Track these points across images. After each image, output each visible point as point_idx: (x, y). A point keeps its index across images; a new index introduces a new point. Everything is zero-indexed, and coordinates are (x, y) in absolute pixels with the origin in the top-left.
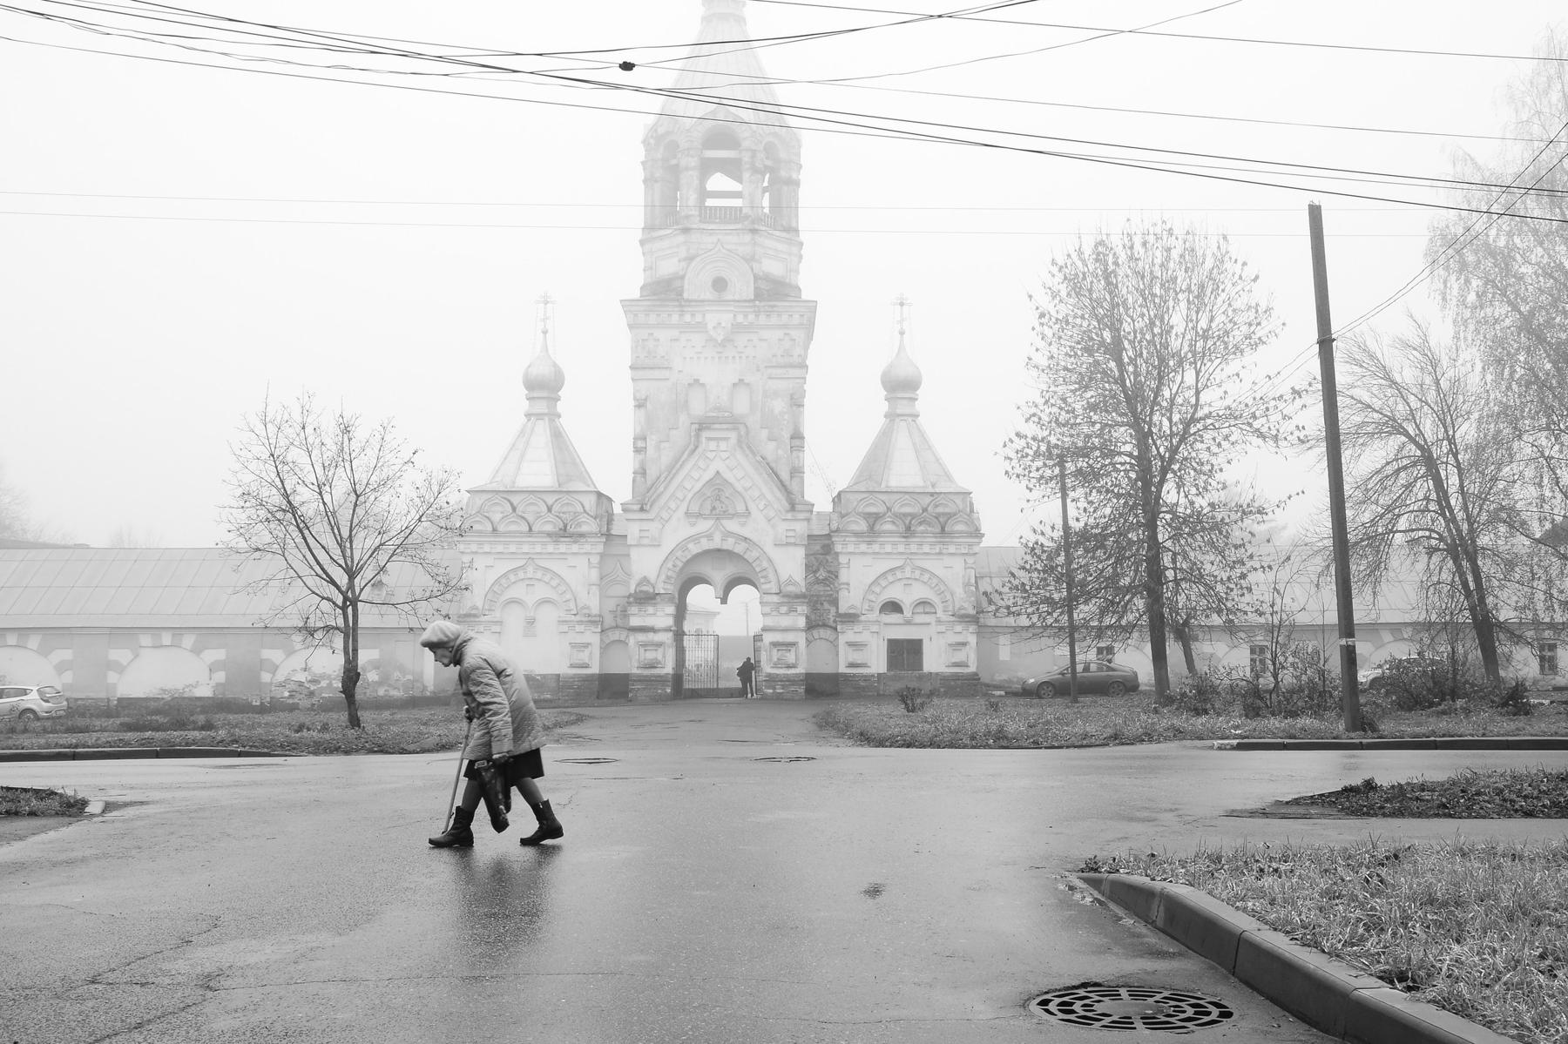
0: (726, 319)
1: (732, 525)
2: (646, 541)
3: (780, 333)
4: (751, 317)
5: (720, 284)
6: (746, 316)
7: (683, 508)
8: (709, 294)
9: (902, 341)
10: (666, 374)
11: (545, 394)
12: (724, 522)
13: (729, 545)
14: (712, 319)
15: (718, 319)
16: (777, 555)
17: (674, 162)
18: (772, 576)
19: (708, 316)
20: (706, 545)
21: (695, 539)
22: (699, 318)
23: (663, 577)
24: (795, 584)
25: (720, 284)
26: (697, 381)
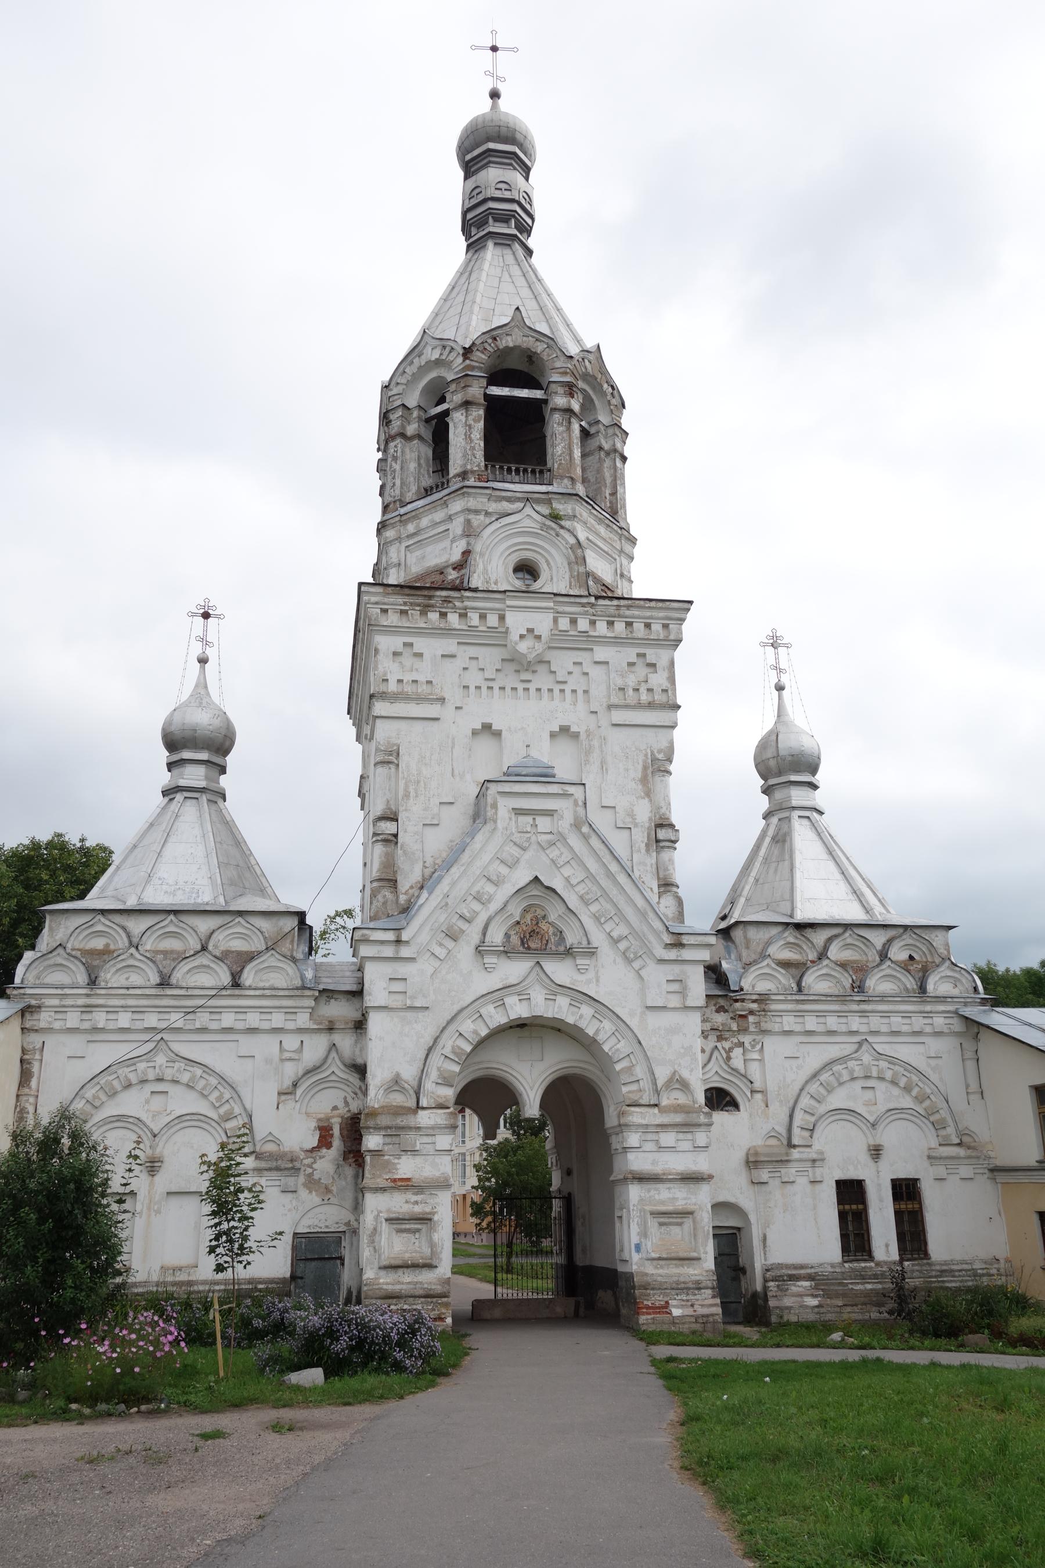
3: (630, 654)
4: (583, 624)
5: (526, 569)
6: (574, 622)
13: (561, 1009)
14: (517, 622)
16: (653, 1029)
17: (440, 409)
18: (640, 1072)
19: (511, 618)
20: (518, 1010)
21: (497, 996)
22: (493, 620)
23: (434, 1075)
24: (684, 1086)
25: (526, 569)
26: (487, 727)
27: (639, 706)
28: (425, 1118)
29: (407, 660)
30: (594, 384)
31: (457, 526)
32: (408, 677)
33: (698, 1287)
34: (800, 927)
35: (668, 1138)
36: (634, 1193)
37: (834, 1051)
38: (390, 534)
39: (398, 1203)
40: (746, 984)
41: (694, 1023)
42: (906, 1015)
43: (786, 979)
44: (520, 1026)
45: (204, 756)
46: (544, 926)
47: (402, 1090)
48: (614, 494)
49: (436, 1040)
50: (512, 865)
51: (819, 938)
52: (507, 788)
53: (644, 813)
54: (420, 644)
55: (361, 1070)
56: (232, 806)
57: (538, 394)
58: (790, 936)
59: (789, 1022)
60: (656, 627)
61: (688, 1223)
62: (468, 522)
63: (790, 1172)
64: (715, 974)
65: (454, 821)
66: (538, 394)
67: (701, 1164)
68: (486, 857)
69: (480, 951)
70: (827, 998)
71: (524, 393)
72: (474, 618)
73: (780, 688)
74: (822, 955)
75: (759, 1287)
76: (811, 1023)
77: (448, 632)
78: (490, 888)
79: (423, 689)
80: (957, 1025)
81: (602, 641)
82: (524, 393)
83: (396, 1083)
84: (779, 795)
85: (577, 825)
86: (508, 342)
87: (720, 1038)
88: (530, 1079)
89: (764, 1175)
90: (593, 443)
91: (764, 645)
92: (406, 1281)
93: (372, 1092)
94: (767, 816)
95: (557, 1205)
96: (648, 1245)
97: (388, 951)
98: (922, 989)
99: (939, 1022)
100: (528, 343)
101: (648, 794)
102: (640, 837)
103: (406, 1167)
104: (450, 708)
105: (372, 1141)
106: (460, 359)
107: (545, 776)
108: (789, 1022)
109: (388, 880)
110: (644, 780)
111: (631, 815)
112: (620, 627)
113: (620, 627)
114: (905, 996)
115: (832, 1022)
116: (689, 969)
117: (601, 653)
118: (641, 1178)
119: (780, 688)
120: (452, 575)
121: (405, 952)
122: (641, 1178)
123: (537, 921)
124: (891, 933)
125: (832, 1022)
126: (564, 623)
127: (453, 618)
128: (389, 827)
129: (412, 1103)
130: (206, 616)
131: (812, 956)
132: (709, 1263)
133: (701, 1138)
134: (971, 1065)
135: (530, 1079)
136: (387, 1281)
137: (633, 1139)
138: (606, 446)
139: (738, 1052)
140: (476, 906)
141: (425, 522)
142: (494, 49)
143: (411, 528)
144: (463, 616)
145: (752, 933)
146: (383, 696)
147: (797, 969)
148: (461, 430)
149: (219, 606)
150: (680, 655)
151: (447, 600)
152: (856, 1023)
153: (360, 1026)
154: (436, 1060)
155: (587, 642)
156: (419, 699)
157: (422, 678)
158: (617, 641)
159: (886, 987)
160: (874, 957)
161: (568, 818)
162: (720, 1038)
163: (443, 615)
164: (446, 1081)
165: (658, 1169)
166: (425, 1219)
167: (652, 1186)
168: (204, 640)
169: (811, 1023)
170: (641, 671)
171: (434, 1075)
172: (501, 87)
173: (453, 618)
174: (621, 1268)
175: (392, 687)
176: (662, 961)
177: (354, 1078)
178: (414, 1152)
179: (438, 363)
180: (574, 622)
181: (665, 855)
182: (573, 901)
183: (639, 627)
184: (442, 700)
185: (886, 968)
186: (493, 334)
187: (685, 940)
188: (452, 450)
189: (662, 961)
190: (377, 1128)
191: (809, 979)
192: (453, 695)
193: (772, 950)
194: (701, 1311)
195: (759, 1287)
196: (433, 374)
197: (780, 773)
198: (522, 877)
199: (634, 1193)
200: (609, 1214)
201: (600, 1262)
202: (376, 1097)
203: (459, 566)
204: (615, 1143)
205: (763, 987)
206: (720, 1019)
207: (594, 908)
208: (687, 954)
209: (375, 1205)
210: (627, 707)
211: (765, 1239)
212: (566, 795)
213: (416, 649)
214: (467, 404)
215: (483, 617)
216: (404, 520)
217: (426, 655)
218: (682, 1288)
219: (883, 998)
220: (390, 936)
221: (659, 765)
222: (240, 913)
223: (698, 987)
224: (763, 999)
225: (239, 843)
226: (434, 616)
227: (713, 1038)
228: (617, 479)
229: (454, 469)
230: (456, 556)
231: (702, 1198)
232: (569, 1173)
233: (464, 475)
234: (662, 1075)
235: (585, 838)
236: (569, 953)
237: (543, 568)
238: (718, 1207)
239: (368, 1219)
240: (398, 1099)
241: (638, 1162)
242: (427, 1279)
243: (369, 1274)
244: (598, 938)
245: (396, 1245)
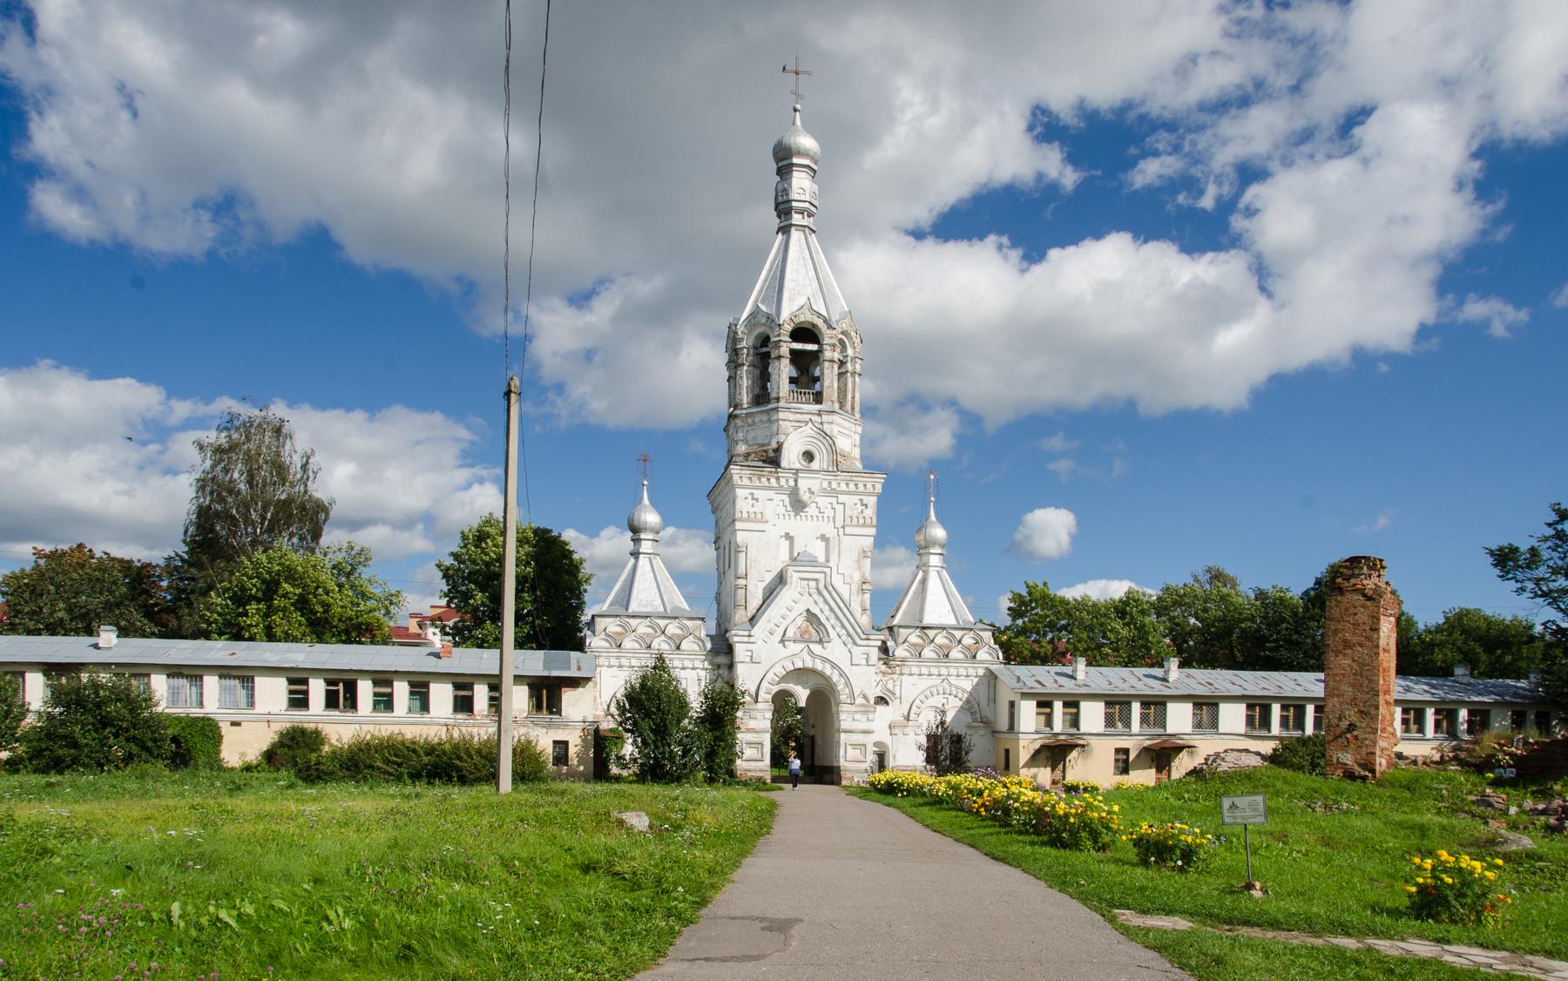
3: (856, 499)
5: (809, 456)
7: (780, 632)
25: (809, 456)
28: (759, 706)
35: (857, 716)
36: (843, 736)
54: (757, 493)
59: (915, 670)
63: (907, 730)
70: (931, 660)
77: (770, 488)
102: (855, 588)
103: (752, 724)
107: (813, 562)
113: (852, 486)
117: (842, 498)
125: (934, 671)
135: (802, 695)
146: (741, 520)
152: (944, 671)
153: (731, 666)
154: (765, 684)
158: (850, 493)
173: (773, 481)
183: (861, 486)
200: (832, 744)
201: (827, 764)
218: (858, 771)
223: (875, 653)
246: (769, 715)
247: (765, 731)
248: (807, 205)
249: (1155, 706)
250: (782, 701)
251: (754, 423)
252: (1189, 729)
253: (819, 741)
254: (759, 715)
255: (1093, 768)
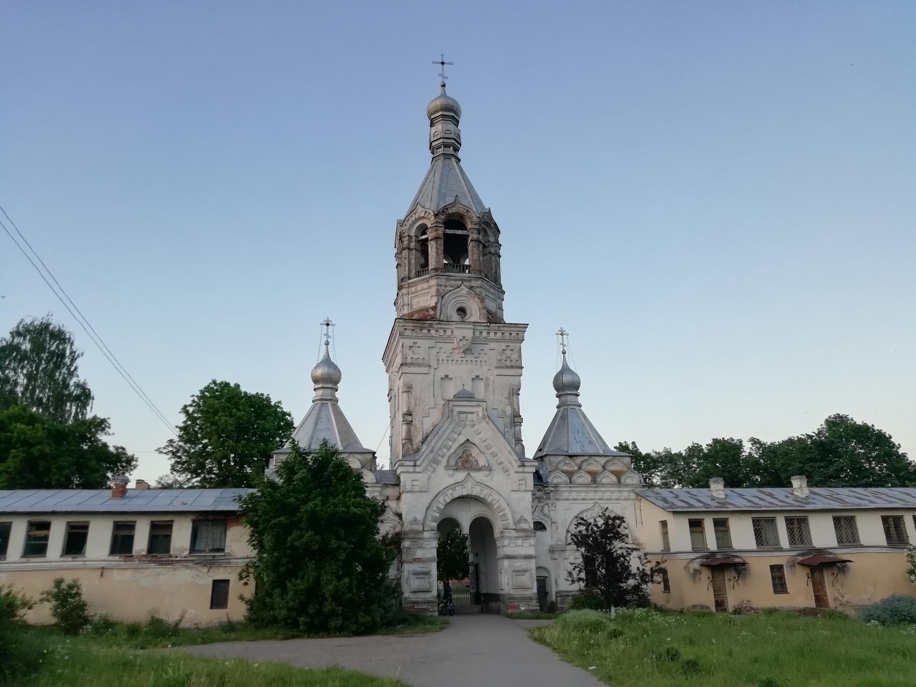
0: (469, 334)
1: (479, 476)
2: (417, 489)
3: (503, 346)
4: (485, 334)
5: (462, 311)
7: (444, 462)
8: (456, 317)
9: (564, 358)
10: (426, 370)
11: (330, 386)
12: (473, 474)
13: (476, 491)
15: (463, 332)
17: (424, 237)
22: (449, 333)
23: (430, 518)
24: (526, 520)
25: (462, 311)
26: (447, 376)
27: (507, 367)
29: (416, 350)
30: (488, 226)
31: (433, 291)
32: (415, 356)
33: (531, 599)
34: (571, 456)
35: (519, 542)
37: (584, 507)
38: (404, 291)
39: (417, 567)
40: (549, 480)
41: (529, 496)
42: (612, 492)
43: (565, 478)
44: (462, 498)
45: (330, 386)
46: (470, 458)
47: (417, 524)
48: (496, 272)
49: (430, 504)
50: (460, 434)
51: (579, 460)
52: (457, 403)
53: (509, 411)
54: (420, 342)
55: (400, 516)
56: (340, 404)
57: (465, 232)
58: (568, 460)
60: (514, 334)
61: (527, 575)
62: (438, 290)
64: (538, 477)
65: (436, 416)
66: (465, 232)
67: (531, 551)
68: (448, 431)
69: (447, 467)
70: (582, 485)
71: (460, 232)
72: (441, 332)
73: (564, 353)
74: (580, 468)
75: (554, 599)
76: (574, 495)
77: (431, 337)
78: (450, 443)
79: (420, 361)
80: (633, 496)
81: (493, 340)
82: (460, 232)
83: (415, 521)
84: (563, 398)
85: (484, 417)
86: (454, 210)
87: (539, 502)
88: (465, 518)
89: (556, 556)
90: (487, 250)
91: (557, 334)
92: (421, 597)
93: (406, 525)
94: (558, 407)
95: (471, 569)
96: (511, 582)
97: (411, 469)
98: (619, 482)
99: (625, 494)
100: (462, 211)
101: (511, 403)
102: (508, 421)
103: (420, 554)
104: (432, 370)
105: (406, 544)
106: (433, 218)
108: (565, 495)
109: (409, 439)
110: (509, 398)
111: (504, 412)
112: (499, 334)
113: (499, 334)
114: (612, 485)
115: (583, 495)
116: (526, 475)
117: (492, 345)
118: (509, 557)
119: (564, 353)
120: (432, 312)
121: (418, 469)
122: (509, 557)
123: (468, 456)
124: (607, 458)
126: (477, 333)
127: (433, 332)
128: (409, 418)
129: (421, 529)
130: (328, 325)
131: (576, 468)
132: (535, 590)
133: (532, 541)
134: (638, 512)
135: (465, 518)
136: (413, 597)
137: (506, 542)
138: (493, 251)
139: (546, 507)
140: (445, 451)
141: (419, 287)
142: (443, 63)
143: (413, 289)
144: (437, 331)
145: (552, 458)
147: (570, 474)
148: (434, 250)
149: (333, 320)
150: (523, 345)
151: (431, 325)
153: (398, 498)
154: (430, 512)
155: (487, 340)
156: (419, 365)
157: (421, 357)
158: (498, 341)
159: (605, 481)
160: (600, 468)
161: (481, 415)
162: (539, 502)
163: (429, 331)
164: (434, 520)
165: (516, 554)
166: (427, 573)
167: (514, 560)
168: (327, 335)
169: (574, 495)
170: (508, 353)
171: (430, 518)
172: (446, 81)
174: (501, 592)
175: (409, 361)
176: (517, 472)
177: (397, 519)
178: (422, 548)
179: (423, 218)
180: (481, 333)
181: (517, 428)
182: (482, 446)
183: (507, 334)
184: (430, 366)
185: (607, 473)
186: (446, 208)
187: (526, 464)
188: (430, 257)
189: (517, 472)
190: (409, 539)
191: (574, 478)
192: (434, 364)
193: (560, 466)
194: (531, 608)
195: (554, 599)
196: (420, 222)
197: (564, 390)
198: (462, 439)
199: (506, 563)
201: (492, 590)
202: (407, 527)
203: (434, 308)
204: (498, 543)
205: (556, 481)
206: (539, 494)
207: (491, 451)
208: (527, 469)
209: (407, 567)
210: (502, 367)
211: (556, 581)
212: (479, 406)
213: (418, 345)
214: (436, 238)
215: (445, 331)
216: (409, 286)
217: (423, 347)
218: (523, 599)
219: (604, 485)
220: (412, 463)
221: (515, 392)
222: (351, 453)
224: (556, 486)
225: (345, 422)
226: (425, 331)
227: (536, 501)
228: (498, 265)
229: (430, 267)
230: (433, 304)
231: (532, 564)
232: (477, 555)
233: (436, 269)
234: (518, 517)
235: (487, 423)
236: (480, 469)
237: (468, 311)
238: (538, 568)
239: (405, 574)
240: (415, 527)
241: (509, 551)
242: (428, 596)
243: (406, 595)
244: (493, 462)
245: (416, 583)
246: (435, 544)
247: (430, 560)
248: (453, 141)
249: (798, 523)
250: (447, 526)
251: (416, 292)
252: (835, 543)
253: (482, 568)
254: (425, 544)
255: (756, 591)
